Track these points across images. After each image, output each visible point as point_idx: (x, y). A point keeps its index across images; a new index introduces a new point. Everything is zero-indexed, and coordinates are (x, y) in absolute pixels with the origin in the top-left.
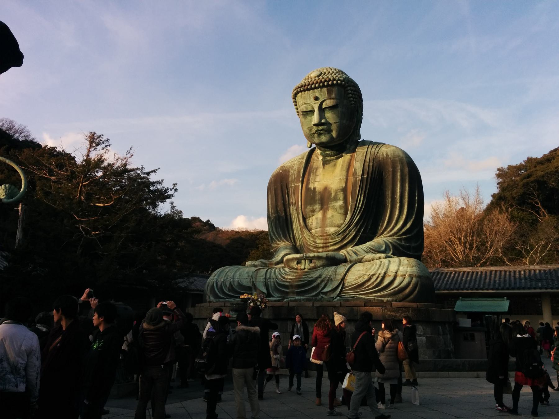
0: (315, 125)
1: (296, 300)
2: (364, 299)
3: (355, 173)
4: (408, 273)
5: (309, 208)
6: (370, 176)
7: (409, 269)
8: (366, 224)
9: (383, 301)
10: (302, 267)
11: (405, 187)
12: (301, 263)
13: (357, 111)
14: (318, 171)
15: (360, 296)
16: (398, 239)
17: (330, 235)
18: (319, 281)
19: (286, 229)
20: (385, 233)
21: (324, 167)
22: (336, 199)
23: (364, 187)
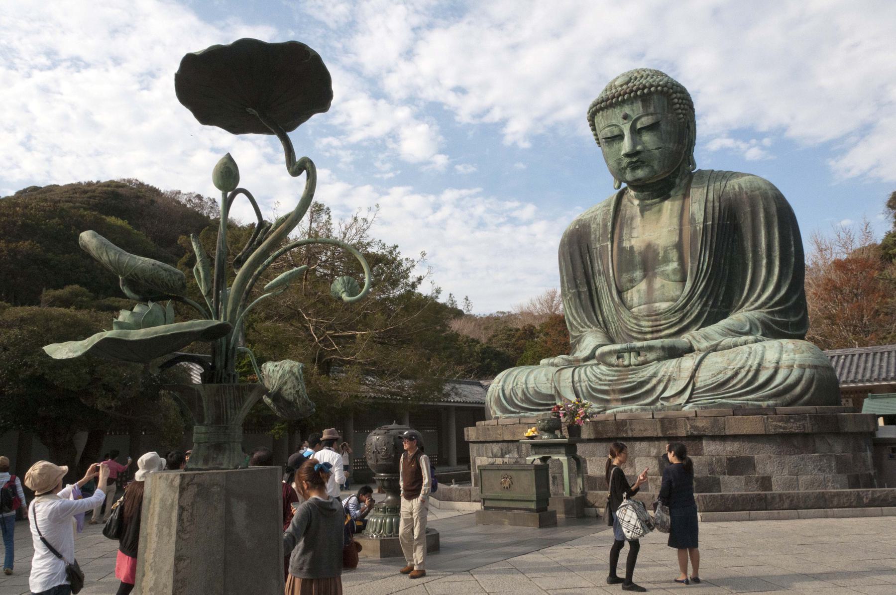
0: (627, 155)
1: (625, 411)
2: (732, 404)
3: (693, 220)
4: (797, 363)
5: (625, 277)
6: (716, 222)
7: (797, 356)
8: (717, 293)
9: (760, 406)
10: (626, 363)
11: (774, 233)
12: (623, 357)
13: (688, 127)
15: (724, 401)
16: (768, 313)
17: (661, 313)
18: (654, 381)
19: (591, 309)
20: (747, 305)
21: (642, 216)
22: (666, 260)
23: (709, 239)
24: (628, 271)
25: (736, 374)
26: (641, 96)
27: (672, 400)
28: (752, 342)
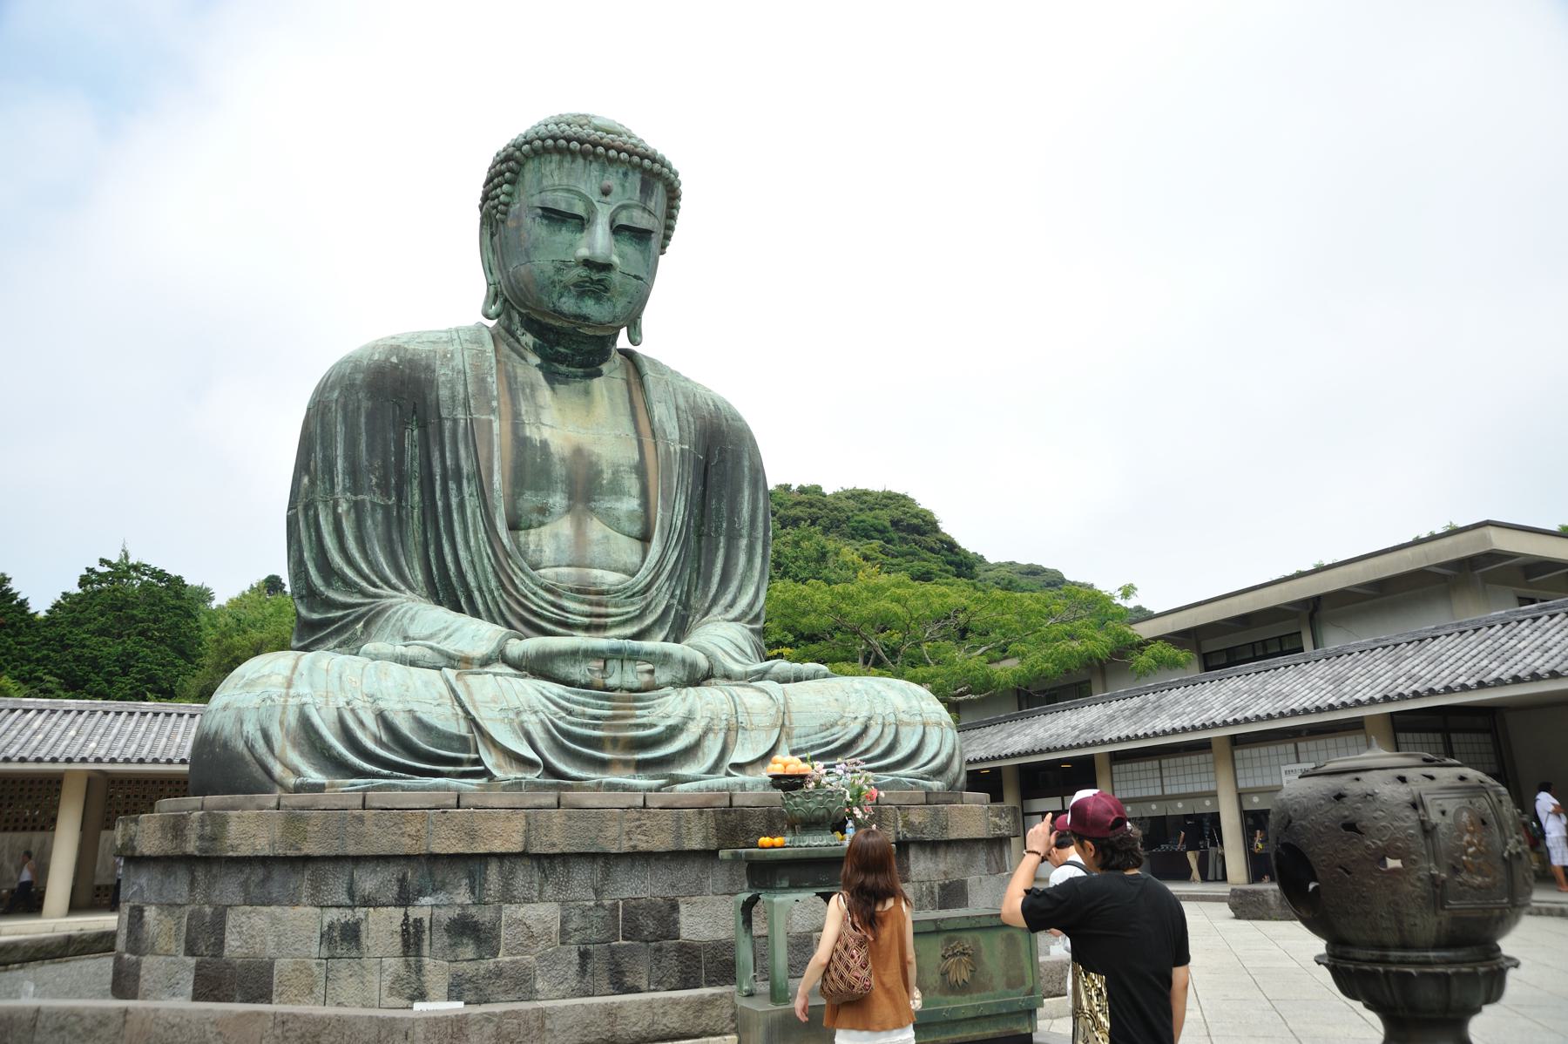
5: (529, 500)
14: (538, 394)
17: (607, 592)
19: (400, 551)
20: (716, 610)
21: (553, 389)
22: (616, 490)
24: (537, 488)
25: (865, 729)
26: (645, 171)
27: (749, 770)
28: (826, 676)
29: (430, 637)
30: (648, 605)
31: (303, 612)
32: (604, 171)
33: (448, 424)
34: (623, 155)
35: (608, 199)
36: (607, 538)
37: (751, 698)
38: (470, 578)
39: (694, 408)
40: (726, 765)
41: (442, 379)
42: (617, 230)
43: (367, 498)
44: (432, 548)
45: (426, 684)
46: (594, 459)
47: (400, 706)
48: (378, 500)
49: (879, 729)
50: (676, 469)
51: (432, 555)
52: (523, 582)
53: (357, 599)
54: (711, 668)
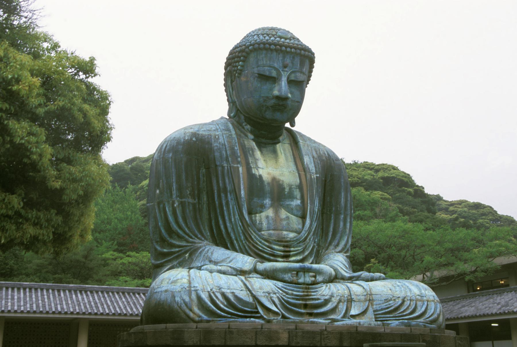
3: (305, 169)
14: (255, 153)
20: (331, 247)
22: (291, 197)
25: (403, 301)
26: (301, 55)
27: (357, 318)
28: (384, 279)
29: (223, 261)
30: (306, 246)
31: (159, 248)
32: (284, 57)
33: (220, 168)
34: (293, 50)
35: (286, 69)
36: (288, 218)
37: (356, 288)
38: (232, 235)
39: (320, 157)
40: (348, 315)
41: (216, 148)
42: (290, 82)
43: (186, 200)
44: (213, 221)
45: (236, 282)
46: (281, 182)
47: (229, 291)
48: (191, 200)
49: (409, 302)
50: (315, 186)
51: (213, 224)
52: (255, 237)
53: (184, 244)
54: (336, 275)
